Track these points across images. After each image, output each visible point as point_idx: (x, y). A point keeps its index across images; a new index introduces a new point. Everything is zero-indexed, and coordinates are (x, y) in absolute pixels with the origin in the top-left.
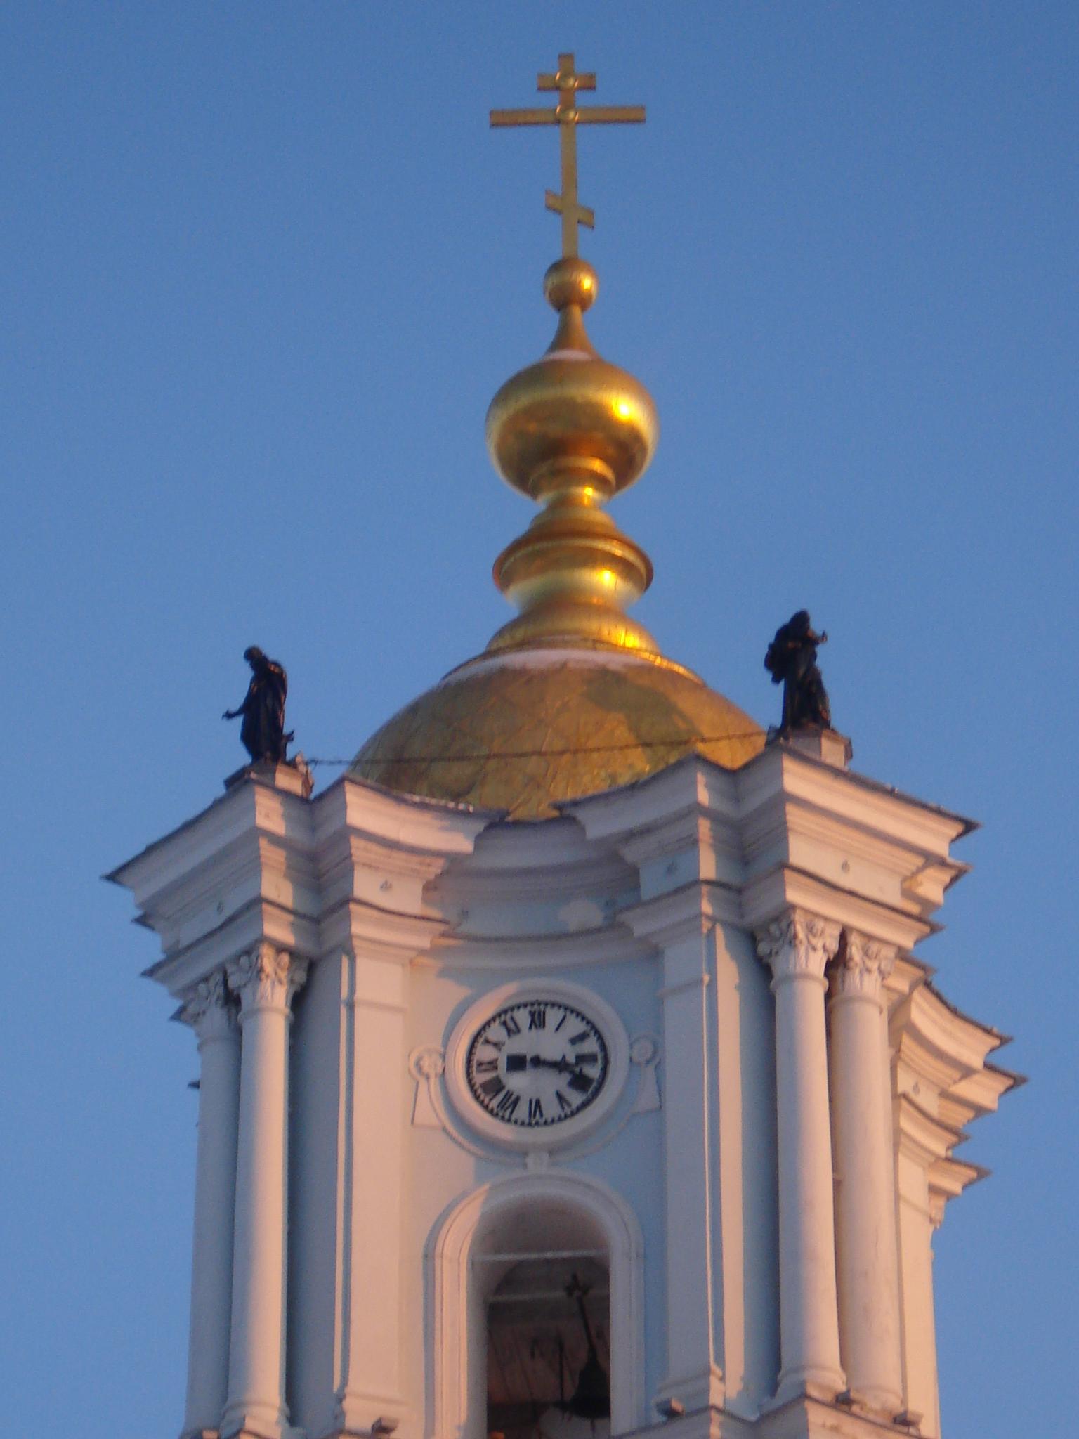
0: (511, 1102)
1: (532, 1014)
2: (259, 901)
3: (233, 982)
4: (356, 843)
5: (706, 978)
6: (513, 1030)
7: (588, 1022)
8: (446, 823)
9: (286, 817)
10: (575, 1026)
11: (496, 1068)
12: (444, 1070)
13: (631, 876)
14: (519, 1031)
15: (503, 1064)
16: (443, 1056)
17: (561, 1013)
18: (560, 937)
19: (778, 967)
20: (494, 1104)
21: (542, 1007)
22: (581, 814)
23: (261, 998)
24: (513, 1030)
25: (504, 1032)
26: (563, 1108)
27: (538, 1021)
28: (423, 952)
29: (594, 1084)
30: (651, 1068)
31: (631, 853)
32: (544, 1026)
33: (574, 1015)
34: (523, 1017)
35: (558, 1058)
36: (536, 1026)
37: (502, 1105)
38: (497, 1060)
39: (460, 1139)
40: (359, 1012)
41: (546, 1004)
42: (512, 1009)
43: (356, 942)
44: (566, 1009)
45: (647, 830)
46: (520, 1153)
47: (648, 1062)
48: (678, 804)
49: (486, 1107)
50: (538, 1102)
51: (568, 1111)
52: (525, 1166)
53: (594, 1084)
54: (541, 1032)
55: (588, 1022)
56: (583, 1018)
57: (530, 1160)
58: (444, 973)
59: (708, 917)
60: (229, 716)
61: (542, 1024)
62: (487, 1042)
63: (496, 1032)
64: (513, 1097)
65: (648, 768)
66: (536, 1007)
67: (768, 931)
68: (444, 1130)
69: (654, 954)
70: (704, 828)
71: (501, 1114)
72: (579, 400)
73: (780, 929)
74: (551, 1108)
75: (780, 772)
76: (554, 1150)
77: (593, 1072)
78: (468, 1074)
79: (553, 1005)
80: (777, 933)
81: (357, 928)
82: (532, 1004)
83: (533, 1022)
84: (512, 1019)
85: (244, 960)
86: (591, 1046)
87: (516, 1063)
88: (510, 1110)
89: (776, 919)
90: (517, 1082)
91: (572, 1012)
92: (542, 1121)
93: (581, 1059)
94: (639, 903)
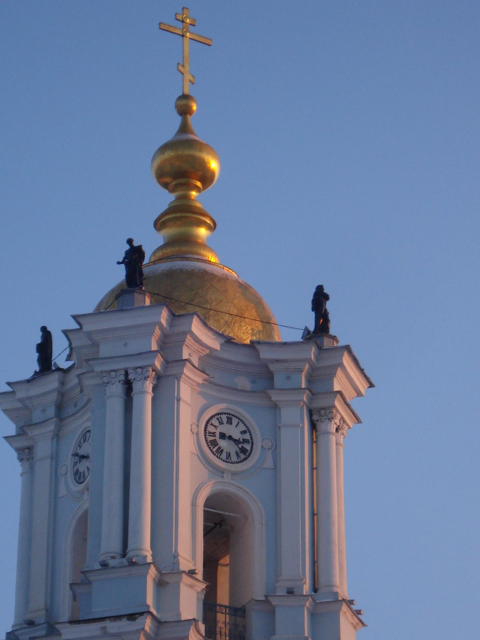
0: (220, 451)
1: (228, 418)
3: (131, 377)
4: (189, 337)
5: (301, 425)
6: (221, 423)
7: (247, 427)
8: (214, 337)
9: (167, 320)
10: (242, 427)
11: (215, 436)
12: (198, 431)
13: (270, 376)
14: (223, 424)
15: (218, 435)
16: (198, 426)
18: (235, 390)
19: (321, 426)
20: (215, 450)
22: (258, 347)
23: (146, 387)
24: (221, 423)
26: (238, 459)
27: (230, 421)
28: (198, 384)
29: (249, 452)
30: (270, 452)
31: (272, 367)
34: (224, 418)
35: (238, 439)
37: (217, 451)
38: (215, 433)
39: (202, 460)
40: (182, 404)
41: (232, 415)
42: (220, 414)
44: (239, 419)
45: (284, 361)
46: (222, 472)
47: (269, 449)
48: (303, 356)
49: (211, 450)
50: (229, 453)
51: (240, 460)
52: (223, 477)
53: (249, 452)
54: (231, 425)
55: (247, 427)
56: (245, 425)
57: (225, 475)
58: (200, 393)
59: (304, 403)
60: (119, 263)
61: (231, 423)
62: (212, 424)
63: (215, 422)
64: (221, 450)
65: (262, 329)
67: (319, 412)
68: (197, 455)
69: (275, 407)
70: (307, 366)
71: (216, 455)
72: (206, 160)
73: (325, 413)
74: (234, 458)
75: (342, 356)
76: (234, 474)
77: (247, 447)
78: (205, 435)
79: (235, 416)
80: (324, 414)
81: (186, 371)
82: (228, 414)
83: (228, 421)
84: (220, 417)
85: (139, 370)
86: (247, 436)
87: (223, 436)
89: (323, 409)
90: (223, 444)
91: (241, 421)
92: (231, 461)
93: (245, 441)
94: (272, 387)
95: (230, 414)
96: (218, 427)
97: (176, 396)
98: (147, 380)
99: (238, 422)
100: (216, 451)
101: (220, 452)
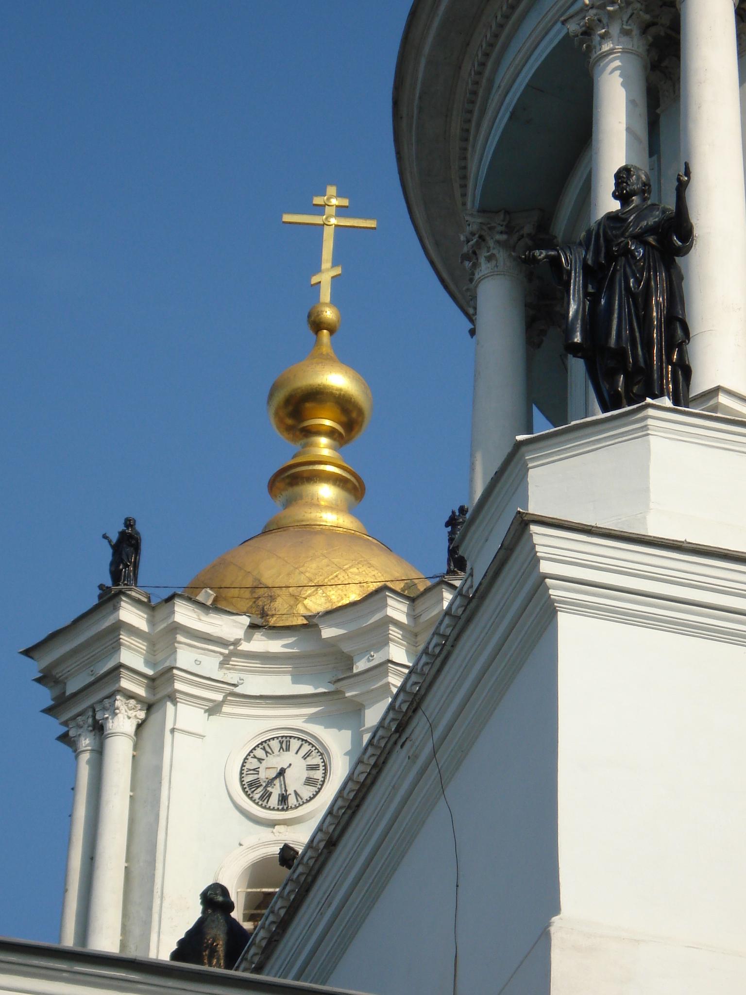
2: (121, 666)
14: (273, 753)
17: (300, 742)
20: (257, 796)
21: (288, 739)
25: (264, 752)
26: (297, 801)
32: (289, 750)
33: (307, 744)
34: (275, 744)
36: (283, 751)
37: (261, 798)
43: (178, 695)
44: (303, 740)
61: (288, 749)
62: (255, 757)
63: (260, 753)
66: (284, 739)
81: (178, 686)
82: (282, 737)
83: (281, 747)
84: (268, 745)
88: (266, 801)
95: (286, 737)
96: (263, 760)
97: (169, 725)
98: (116, 714)
99: (302, 745)
100: (259, 799)
101: (266, 798)
